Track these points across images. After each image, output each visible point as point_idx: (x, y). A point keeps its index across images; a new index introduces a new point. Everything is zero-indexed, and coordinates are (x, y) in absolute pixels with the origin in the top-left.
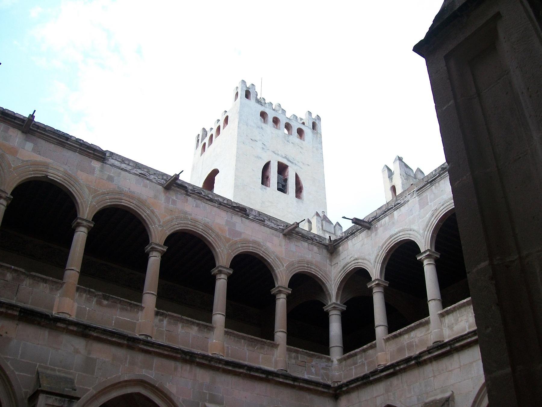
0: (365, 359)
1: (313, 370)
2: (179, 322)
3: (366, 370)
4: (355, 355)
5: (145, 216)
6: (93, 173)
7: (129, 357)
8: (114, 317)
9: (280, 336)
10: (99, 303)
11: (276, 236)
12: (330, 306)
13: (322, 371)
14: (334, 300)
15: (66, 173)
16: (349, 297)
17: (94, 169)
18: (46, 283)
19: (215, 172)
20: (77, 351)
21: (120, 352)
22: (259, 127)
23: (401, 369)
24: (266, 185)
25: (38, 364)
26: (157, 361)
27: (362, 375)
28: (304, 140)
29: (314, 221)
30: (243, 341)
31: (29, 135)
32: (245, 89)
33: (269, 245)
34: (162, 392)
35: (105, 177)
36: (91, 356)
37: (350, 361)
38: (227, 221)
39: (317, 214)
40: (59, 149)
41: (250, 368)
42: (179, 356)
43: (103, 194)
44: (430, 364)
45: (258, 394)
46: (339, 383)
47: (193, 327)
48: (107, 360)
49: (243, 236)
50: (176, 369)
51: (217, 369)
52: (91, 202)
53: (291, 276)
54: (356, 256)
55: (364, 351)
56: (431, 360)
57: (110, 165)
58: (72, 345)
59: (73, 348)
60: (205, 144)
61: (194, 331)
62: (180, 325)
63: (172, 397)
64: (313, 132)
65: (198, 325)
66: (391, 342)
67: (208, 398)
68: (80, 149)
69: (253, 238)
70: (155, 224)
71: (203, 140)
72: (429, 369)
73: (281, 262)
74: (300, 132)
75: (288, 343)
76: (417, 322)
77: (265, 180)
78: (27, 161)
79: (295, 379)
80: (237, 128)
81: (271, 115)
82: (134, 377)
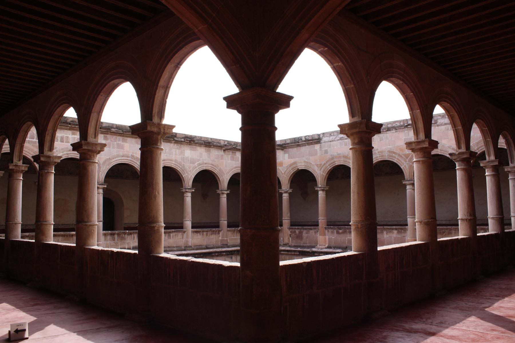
2: (384, 231)
8: (347, 238)
10: (338, 233)
15: (305, 162)
17: (316, 151)
18: (312, 230)
31: (285, 150)
35: (324, 152)
40: (299, 148)
43: (325, 164)
52: (320, 173)
57: (324, 143)
62: (385, 232)
65: (396, 229)
68: (307, 143)
78: (287, 166)
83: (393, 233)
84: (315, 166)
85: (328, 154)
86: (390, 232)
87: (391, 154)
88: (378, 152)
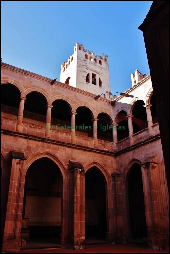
0: (125, 143)
1: (107, 148)
3: (126, 147)
4: (122, 141)
5: (45, 95)
6: (25, 81)
7: (42, 145)
8: (36, 131)
9: (96, 135)
10: (30, 127)
11: (93, 100)
12: (113, 124)
13: (110, 148)
14: (114, 122)
15: (15, 81)
16: (120, 121)
17: (25, 78)
19: (69, 78)
20: (24, 144)
21: (40, 143)
22: (84, 60)
23: (138, 146)
24: (88, 82)
25: (11, 149)
26: (52, 146)
27: (124, 149)
28: (102, 65)
29: (106, 94)
30: (82, 138)
32: (79, 46)
33: (90, 103)
34: (54, 156)
36: (29, 145)
37: (120, 144)
38: (75, 96)
39: (107, 92)
41: (85, 147)
42: (60, 144)
44: (148, 144)
45: (88, 156)
46: (116, 152)
47: (64, 133)
48: (35, 146)
49: (80, 101)
50: (59, 148)
51: (73, 148)
53: (98, 114)
54: (121, 107)
55: (125, 140)
56: (148, 143)
58: (22, 142)
59: (22, 143)
60: (65, 68)
61: (64, 135)
62: (59, 133)
63: (58, 158)
64: (105, 62)
66: (135, 137)
67: (70, 158)
69: (84, 101)
70: (48, 98)
71: (64, 66)
72: (148, 146)
73: (95, 110)
74: (100, 62)
75: (98, 138)
76: (144, 130)
77: (88, 80)
79: (101, 151)
80: (76, 61)
81: (89, 56)
82: (44, 152)
83: (63, 134)
84: (23, 87)
85: (33, 84)
86: (62, 133)
87: (67, 98)
88: (61, 95)
